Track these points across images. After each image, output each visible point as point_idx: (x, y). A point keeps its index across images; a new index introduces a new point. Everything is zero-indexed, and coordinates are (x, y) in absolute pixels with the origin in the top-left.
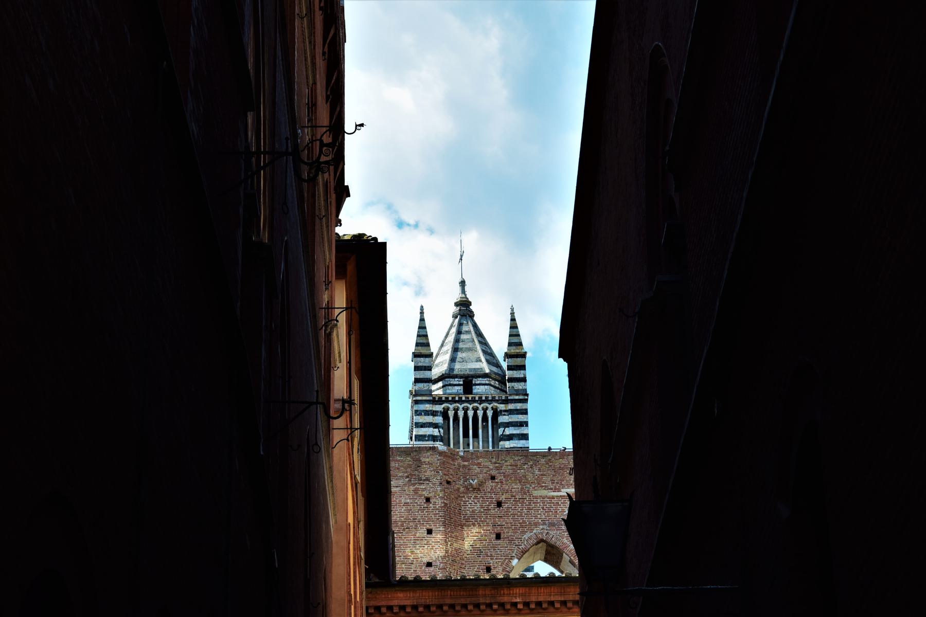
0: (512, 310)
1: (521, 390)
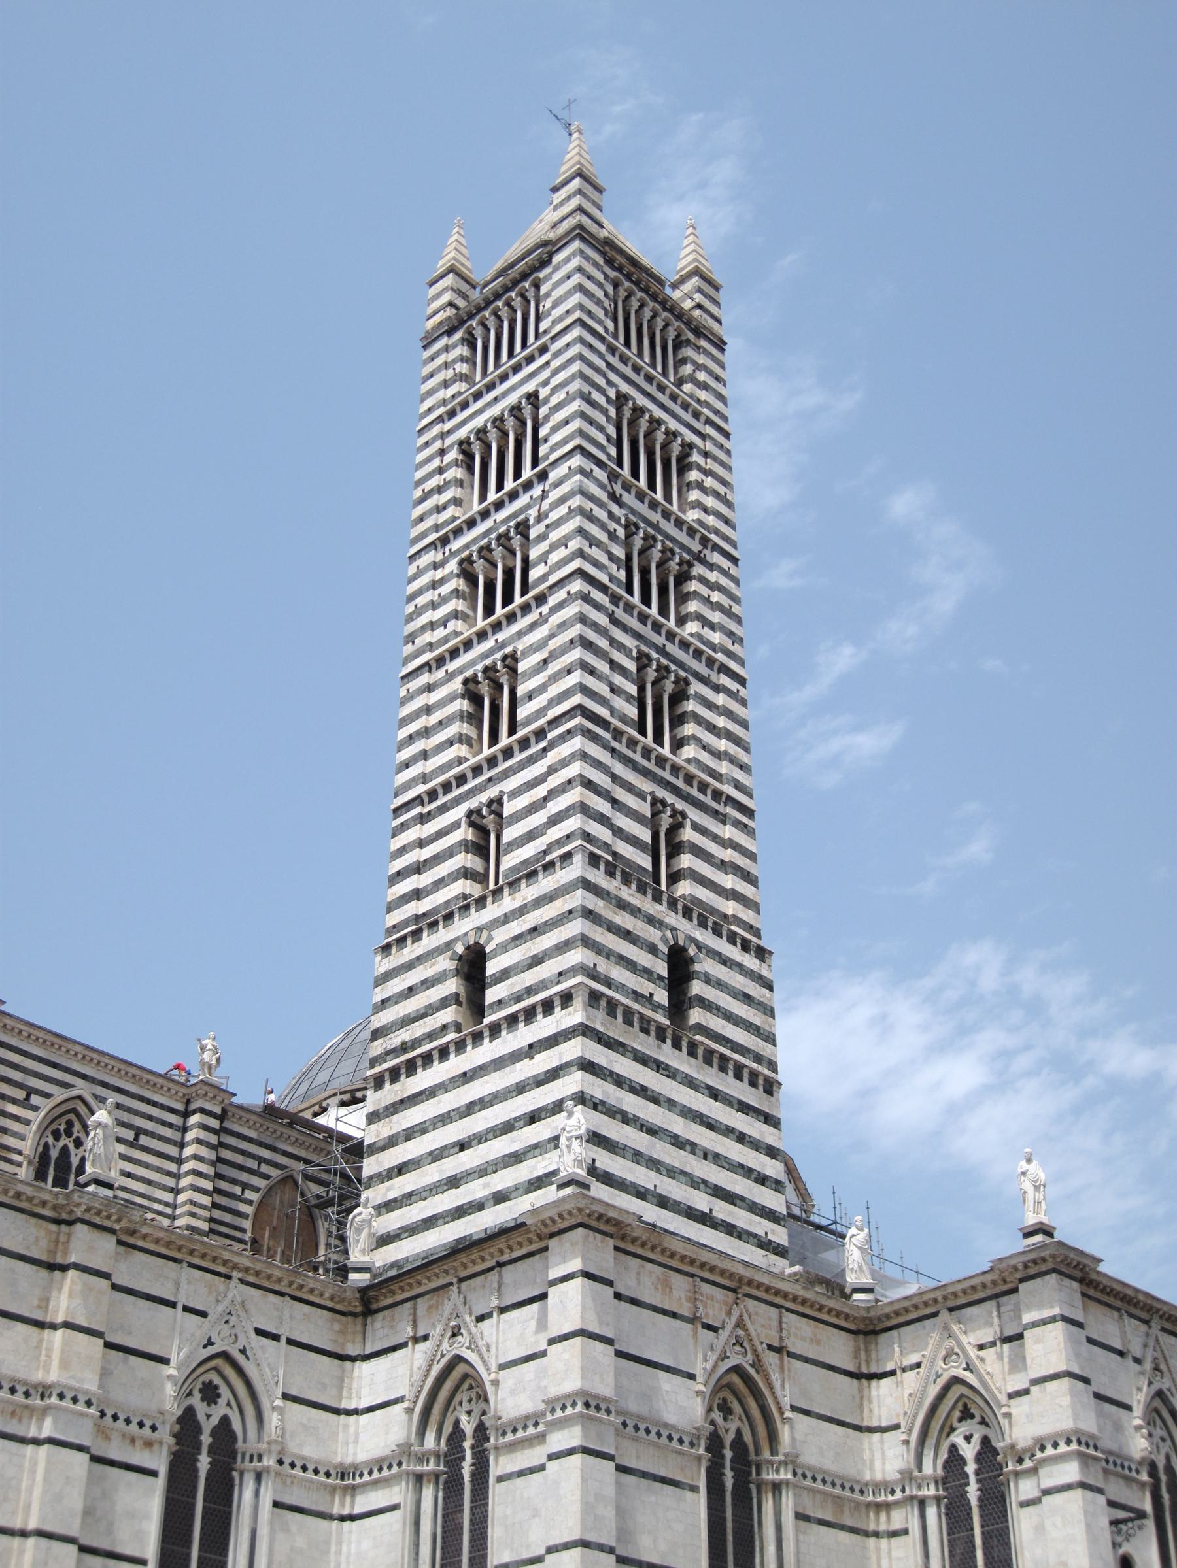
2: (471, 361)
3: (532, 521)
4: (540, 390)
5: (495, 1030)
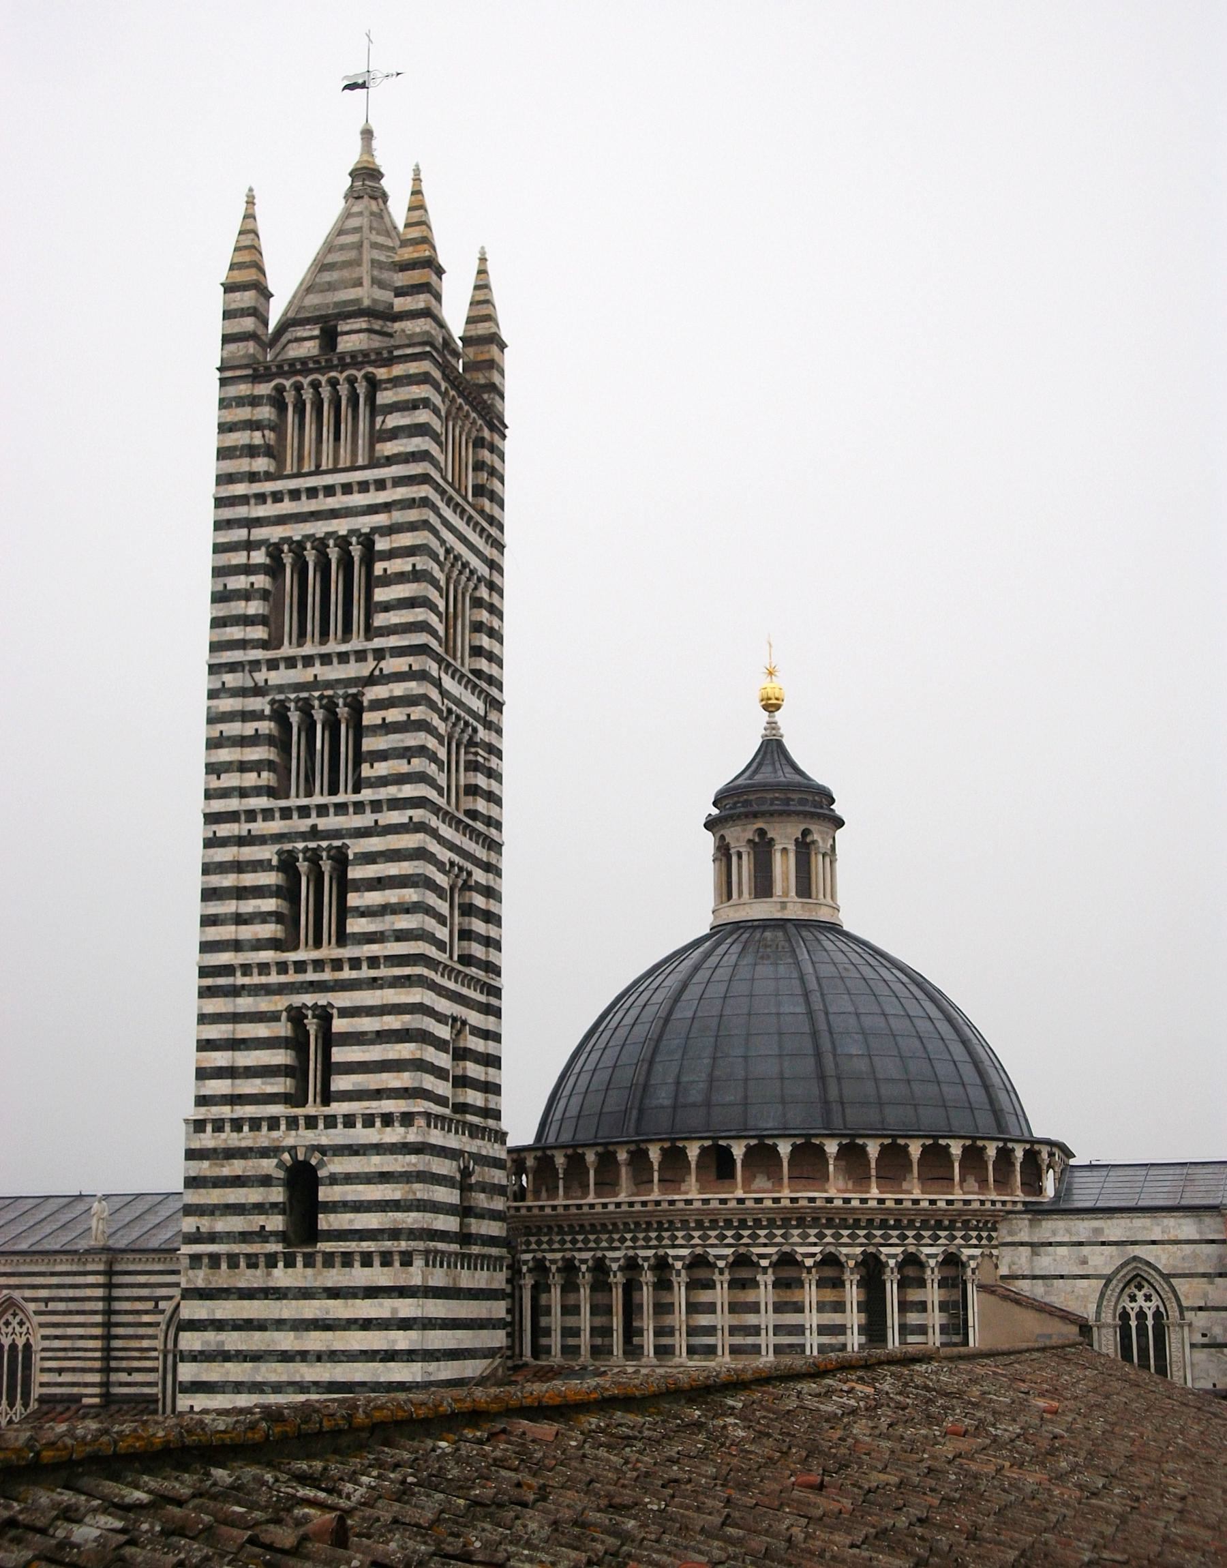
0: (417, 171)
1: (419, 334)
2: (278, 427)
3: (365, 704)
4: (377, 537)
5: (328, 1260)
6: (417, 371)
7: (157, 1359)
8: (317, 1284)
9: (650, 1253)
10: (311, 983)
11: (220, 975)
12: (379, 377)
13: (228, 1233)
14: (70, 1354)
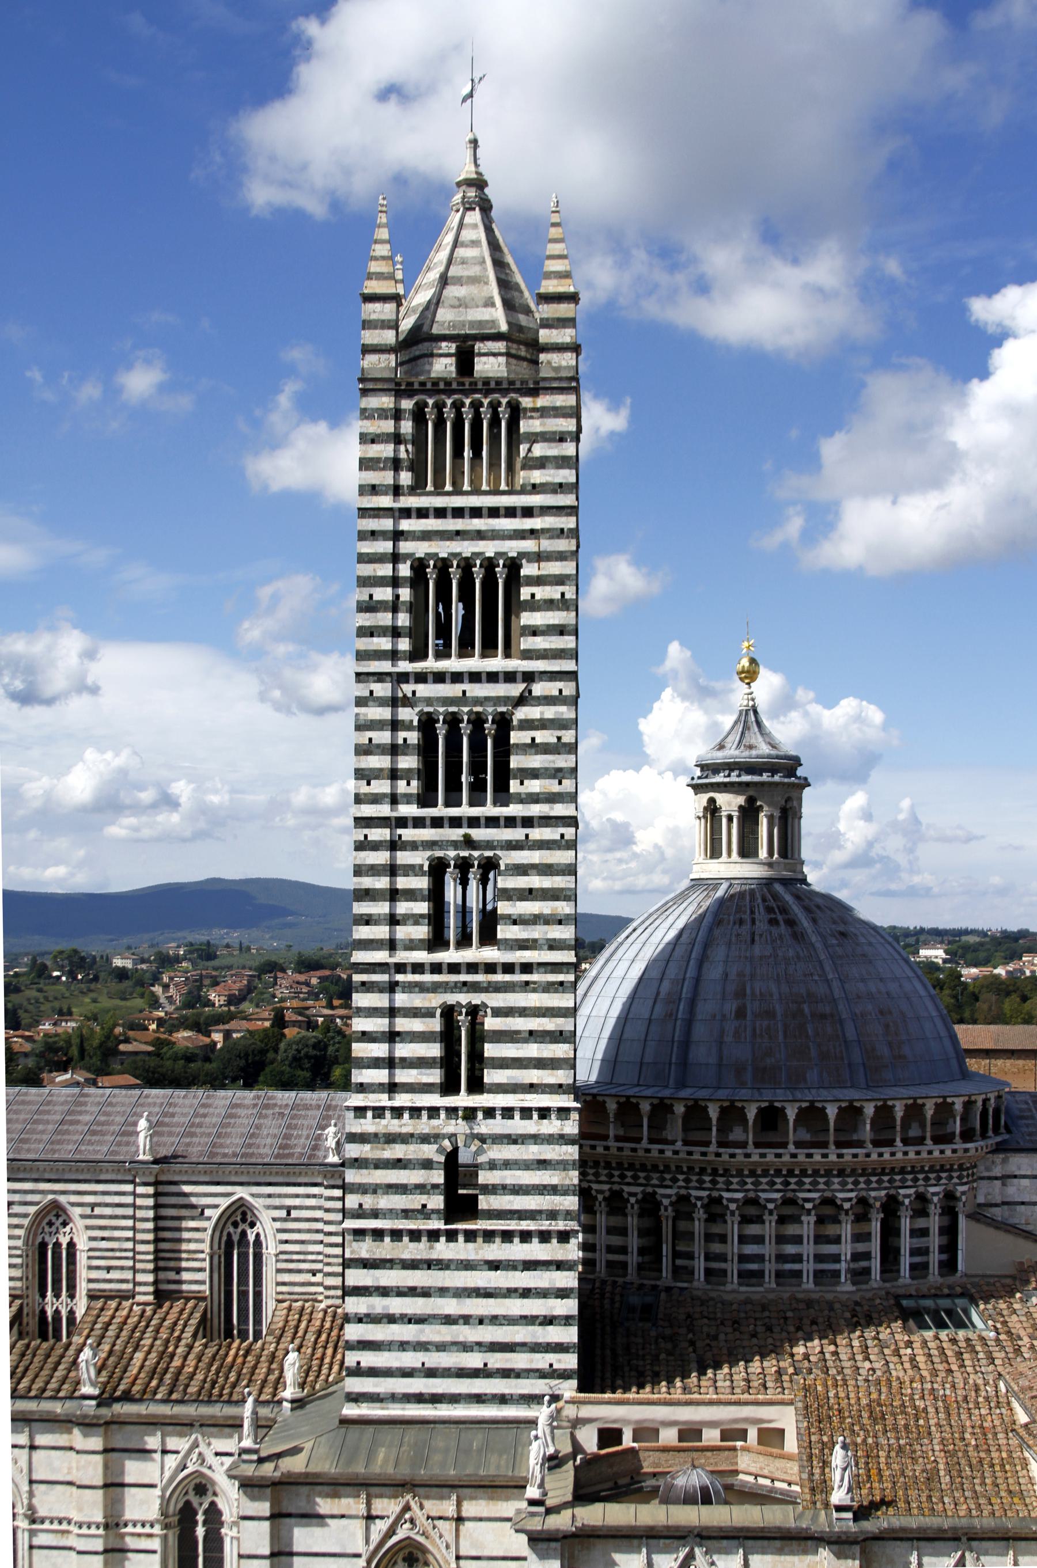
1: (565, 368)
3: (515, 723)
4: (524, 561)
5: (489, 1236)
6: (564, 404)
7: (204, 1260)
8: (479, 1257)
9: (704, 1194)
10: (465, 984)
11: (374, 972)
12: (524, 405)
13: (391, 1210)
14: (118, 1254)
